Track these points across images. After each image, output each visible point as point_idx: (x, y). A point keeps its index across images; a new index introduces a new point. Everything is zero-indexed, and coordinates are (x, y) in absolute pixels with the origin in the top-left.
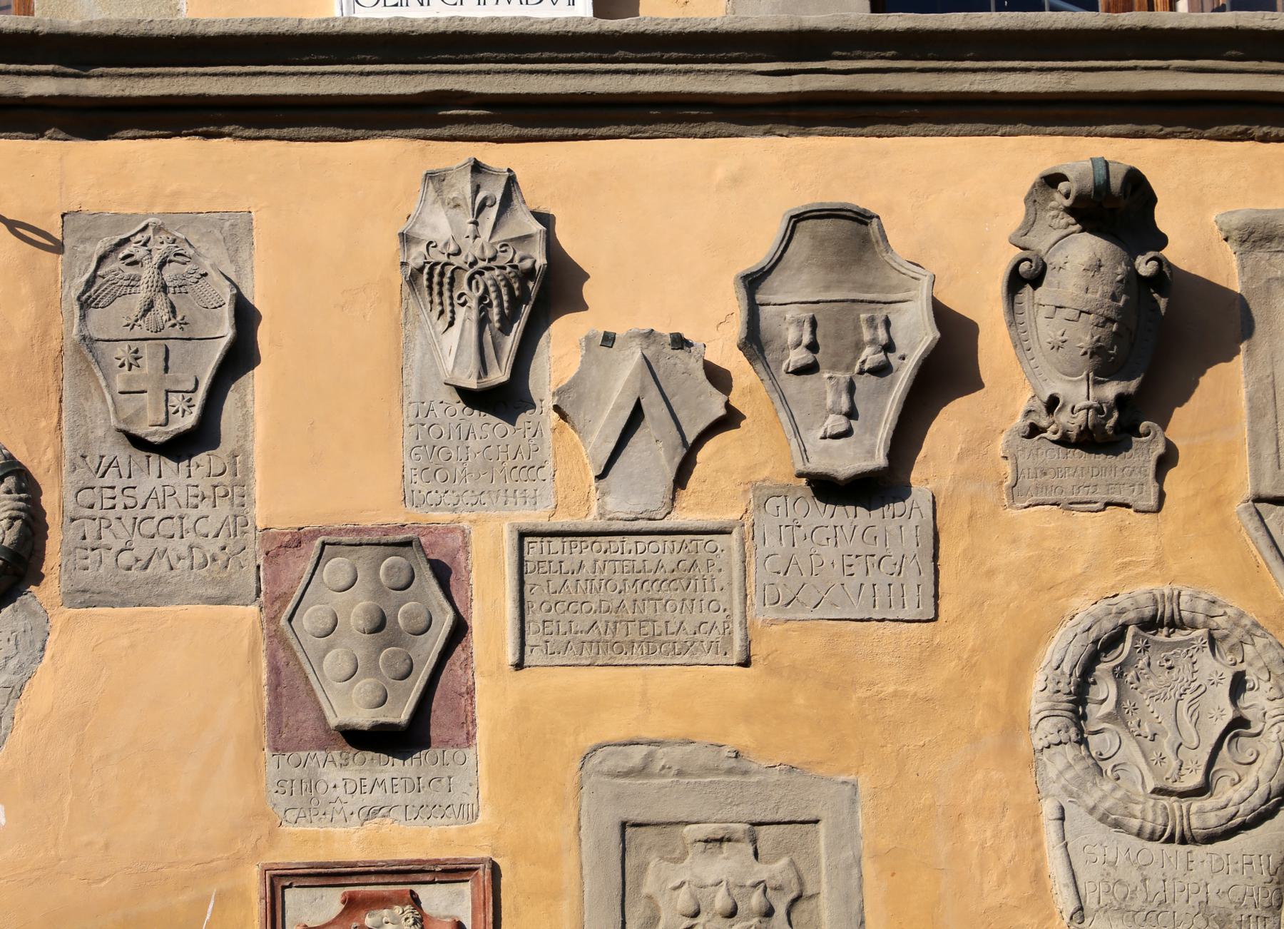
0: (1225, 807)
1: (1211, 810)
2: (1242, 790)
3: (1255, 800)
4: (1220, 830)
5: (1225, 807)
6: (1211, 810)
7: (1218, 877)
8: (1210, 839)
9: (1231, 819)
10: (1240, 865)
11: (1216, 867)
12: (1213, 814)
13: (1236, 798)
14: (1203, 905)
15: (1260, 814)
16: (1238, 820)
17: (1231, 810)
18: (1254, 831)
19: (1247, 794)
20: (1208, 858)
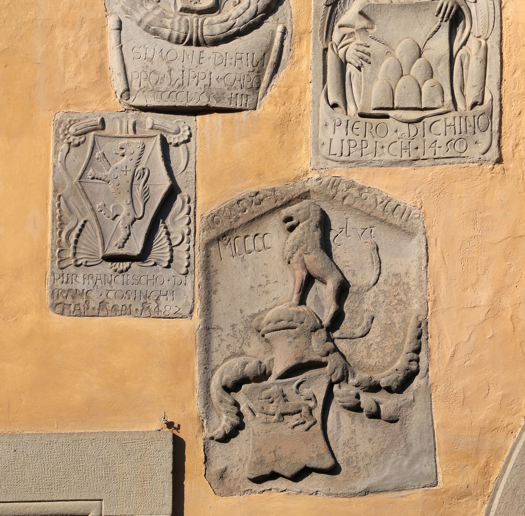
0: (227, 20)
1: (217, 23)
2: (239, 9)
3: (247, 16)
4: (222, 36)
5: (227, 20)
6: (217, 23)
7: (218, 68)
8: (216, 42)
9: (230, 29)
10: (234, 60)
11: (218, 61)
12: (218, 25)
13: (234, 14)
14: (207, 87)
15: (249, 25)
16: (234, 30)
17: (230, 22)
18: (245, 37)
19: (241, 11)
20: (213, 56)
